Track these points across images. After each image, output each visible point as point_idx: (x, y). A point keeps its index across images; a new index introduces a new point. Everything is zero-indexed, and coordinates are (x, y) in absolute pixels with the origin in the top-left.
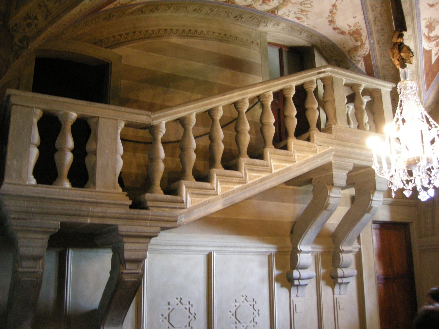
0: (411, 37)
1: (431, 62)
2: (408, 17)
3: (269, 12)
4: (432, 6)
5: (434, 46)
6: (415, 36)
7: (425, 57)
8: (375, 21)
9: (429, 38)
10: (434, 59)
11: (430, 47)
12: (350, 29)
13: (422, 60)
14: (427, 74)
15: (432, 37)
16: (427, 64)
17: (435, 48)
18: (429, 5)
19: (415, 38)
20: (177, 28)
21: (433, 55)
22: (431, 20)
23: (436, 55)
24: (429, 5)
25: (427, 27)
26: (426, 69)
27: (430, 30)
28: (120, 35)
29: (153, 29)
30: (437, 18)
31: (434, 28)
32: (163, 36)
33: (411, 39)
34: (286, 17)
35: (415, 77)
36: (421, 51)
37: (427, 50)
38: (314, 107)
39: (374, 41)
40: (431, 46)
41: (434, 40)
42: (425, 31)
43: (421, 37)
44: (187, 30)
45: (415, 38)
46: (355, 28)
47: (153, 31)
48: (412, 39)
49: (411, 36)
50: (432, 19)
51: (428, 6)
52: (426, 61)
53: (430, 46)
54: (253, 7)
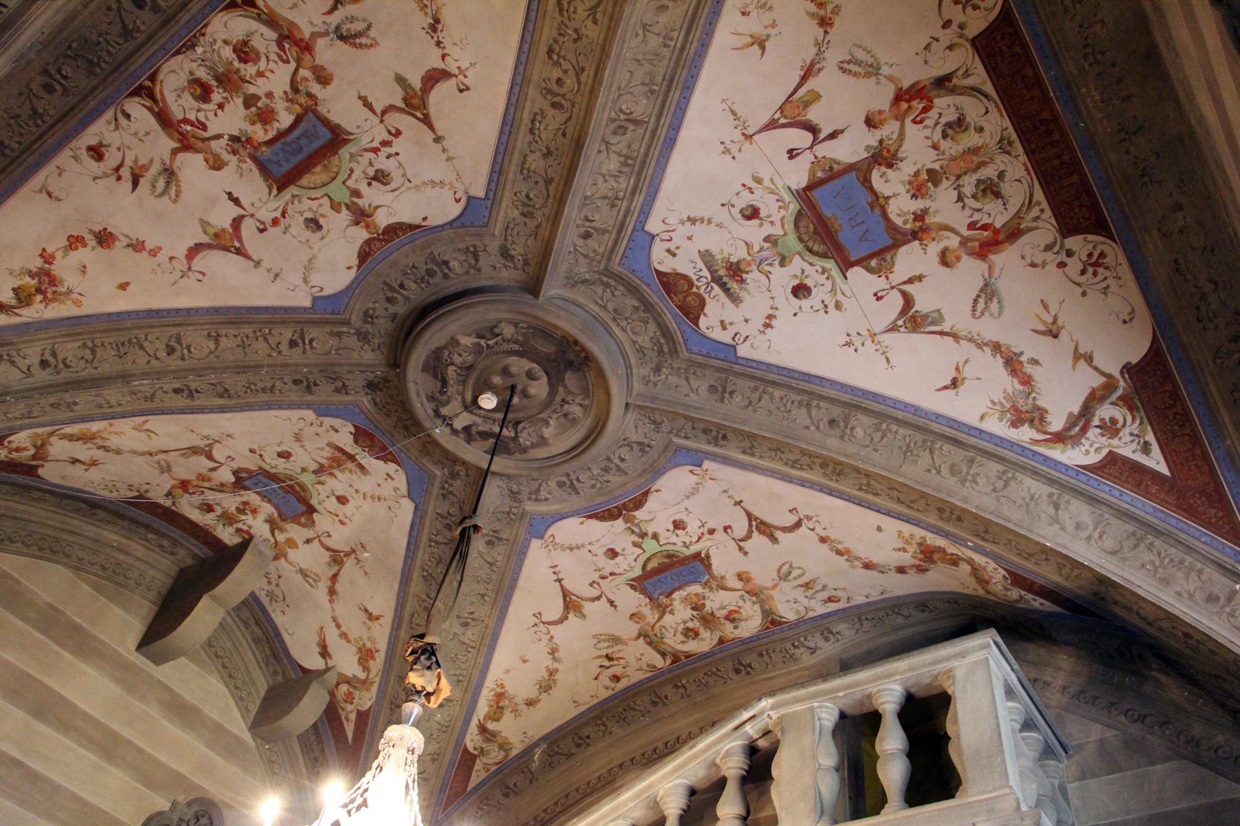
0: (1010, 475)
1: (1155, 475)
2: (941, 448)
3: (768, 628)
4: (955, 384)
5: (1104, 440)
6: (1014, 464)
7: (1117, 479)
8: (909, 507)
9: (1059, 438)
10: (1156, 462)
11: (1098, 450)
12: (910, 553)
13: (1116, 493)
14: (1191, 512)
15: (1067, 428)
16: (1154, 489)
17: (1115, 442)
18: (946, 388)
19: (1024, 468)
20: (642, 751)
21: (1139, 457)
22: (1002, 404)
23: (1146, 449)
24: (946, 388)
25: (1015, 424)
26: (1163, 503)
27: (1036, 422)
28: (545, 811)
29: (597, 774)
30: (1010, 390)
31: (1039, 409)
32: (615, 779)
33: (1014, 478)
34: (811, 614)
35: (1158, 543)
36: (1085, 479)
37: (1101, 461)
38: (1108, 762)
39: (971, 541)
40: (1096, 446)
41: (1084, 429)
42: (1025, 434)
43: (1035, 453)
44: (660, 745)
45: (1024, 468)
46: (915, 546)
47: (599, 778)
48: (1017, 474)
49: (1004, 473)
50: (1004, 401)
51: (950, 392)
52: (1138, 486)
53: (1092, 450)
54: (733, 639)
